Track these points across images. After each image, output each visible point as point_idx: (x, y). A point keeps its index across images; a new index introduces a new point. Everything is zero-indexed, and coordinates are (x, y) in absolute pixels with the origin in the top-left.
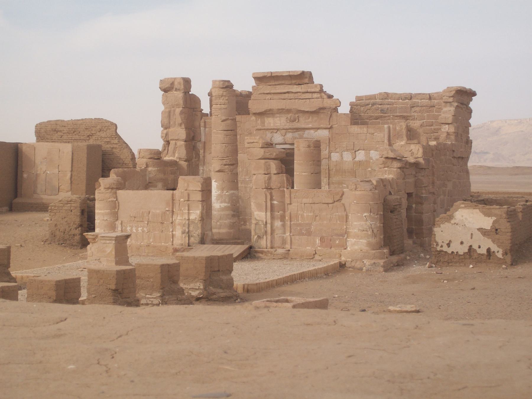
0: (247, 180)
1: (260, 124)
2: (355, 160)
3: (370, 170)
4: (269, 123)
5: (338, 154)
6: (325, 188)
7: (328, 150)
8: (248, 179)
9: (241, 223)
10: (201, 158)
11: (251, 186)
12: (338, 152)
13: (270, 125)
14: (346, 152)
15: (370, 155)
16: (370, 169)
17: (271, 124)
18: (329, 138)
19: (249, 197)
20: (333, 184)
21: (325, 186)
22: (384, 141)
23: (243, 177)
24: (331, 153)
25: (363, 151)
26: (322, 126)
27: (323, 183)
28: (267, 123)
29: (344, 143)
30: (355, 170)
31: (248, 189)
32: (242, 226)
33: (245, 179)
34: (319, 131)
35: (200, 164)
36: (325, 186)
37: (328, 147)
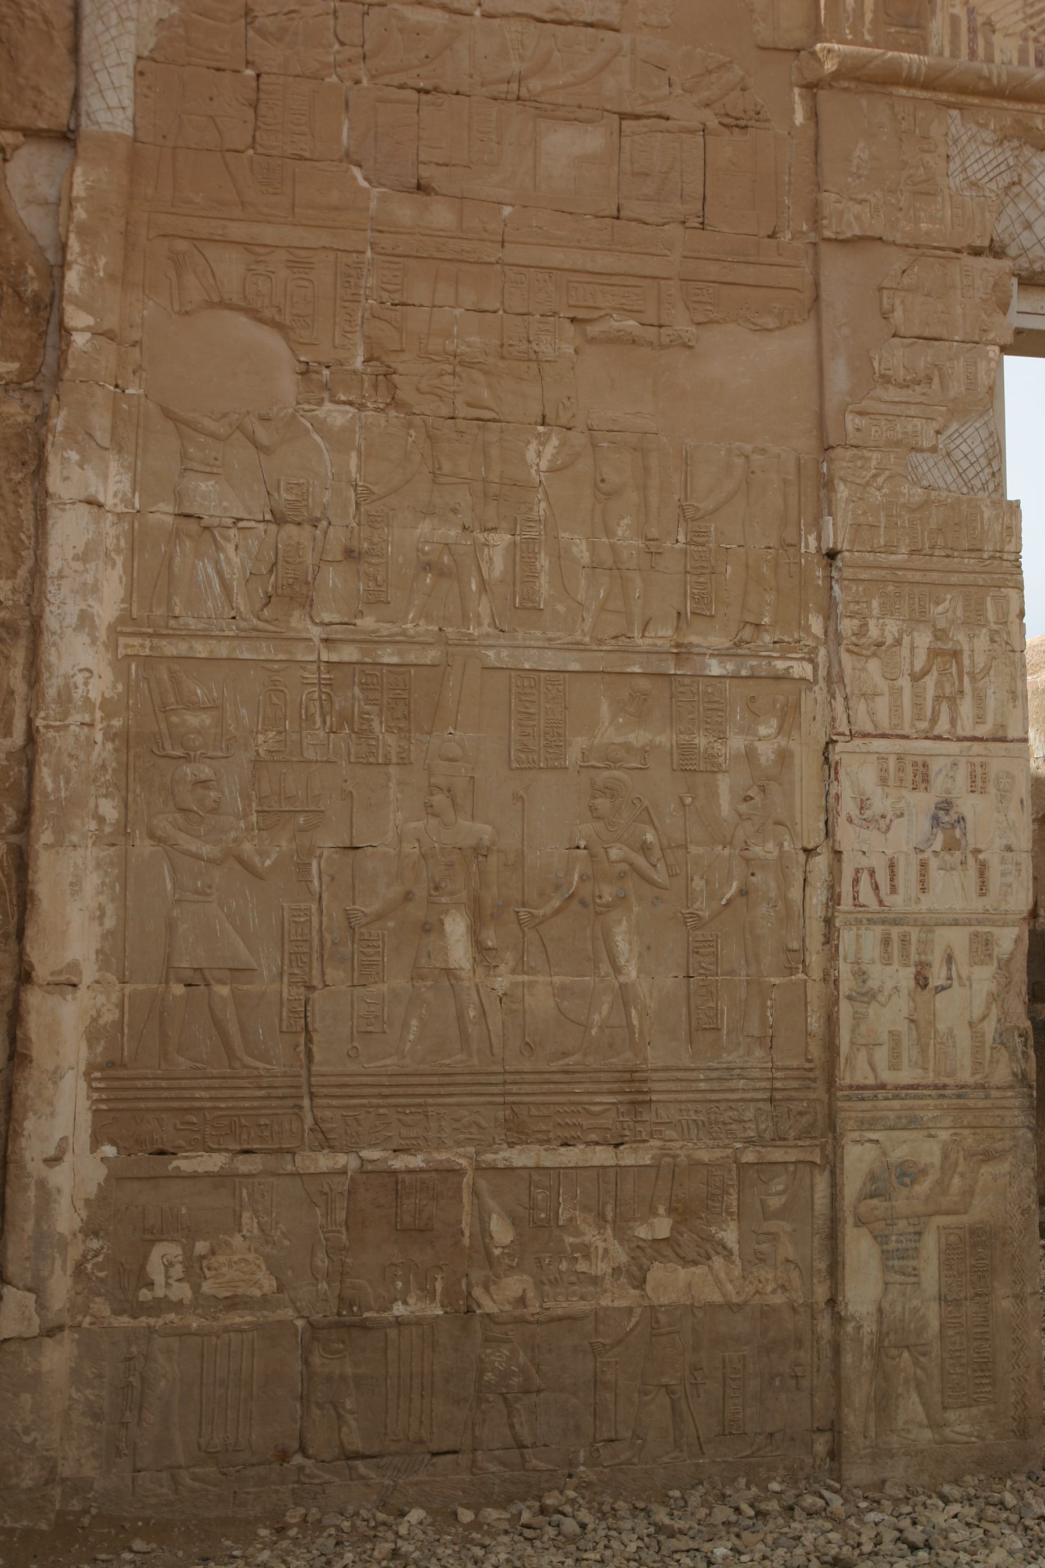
0: (715, 668)
1: (869, 16)
4: (972, 31)
8: (721, 655)
9: (642, 1232)
10: (80, 340)
11: (766, 751)
13: (989, 44)
17: (997, 39)
19: (743, 892)
23: (663, 634)
28: (954, 20)
31: (723, 784)
32: (657, 1272)
33: (682, 653)
35: (59, 422)
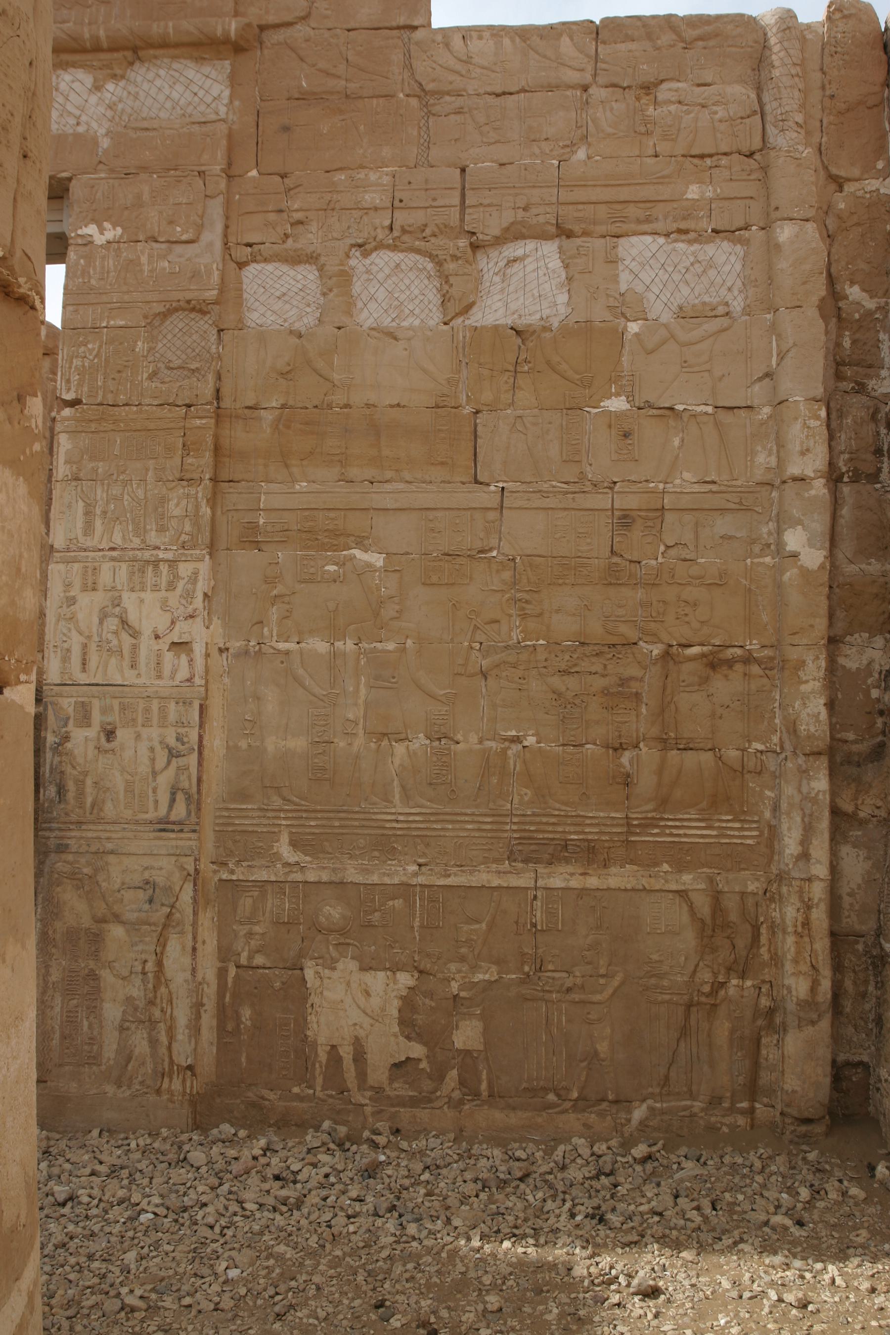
2: (477, 318)
3: (619, 415)
5: (307, 275)
6: (177, 577)
7: (213, 236)
12: (311, 258)
14: (383, 259)
15: (615, 279)
16: (617, 404)
18: (230, 136)
20: (257, 545)
21: (172, 563)
22: (757, 143)
24: (241, 265)
25: (550, 248)
26: (169, 28)
27: (162, 529)
29: (373, 177)
30: (468, 410)
34: (139, 74)
36: (172, 563)
37: (216, 209)
